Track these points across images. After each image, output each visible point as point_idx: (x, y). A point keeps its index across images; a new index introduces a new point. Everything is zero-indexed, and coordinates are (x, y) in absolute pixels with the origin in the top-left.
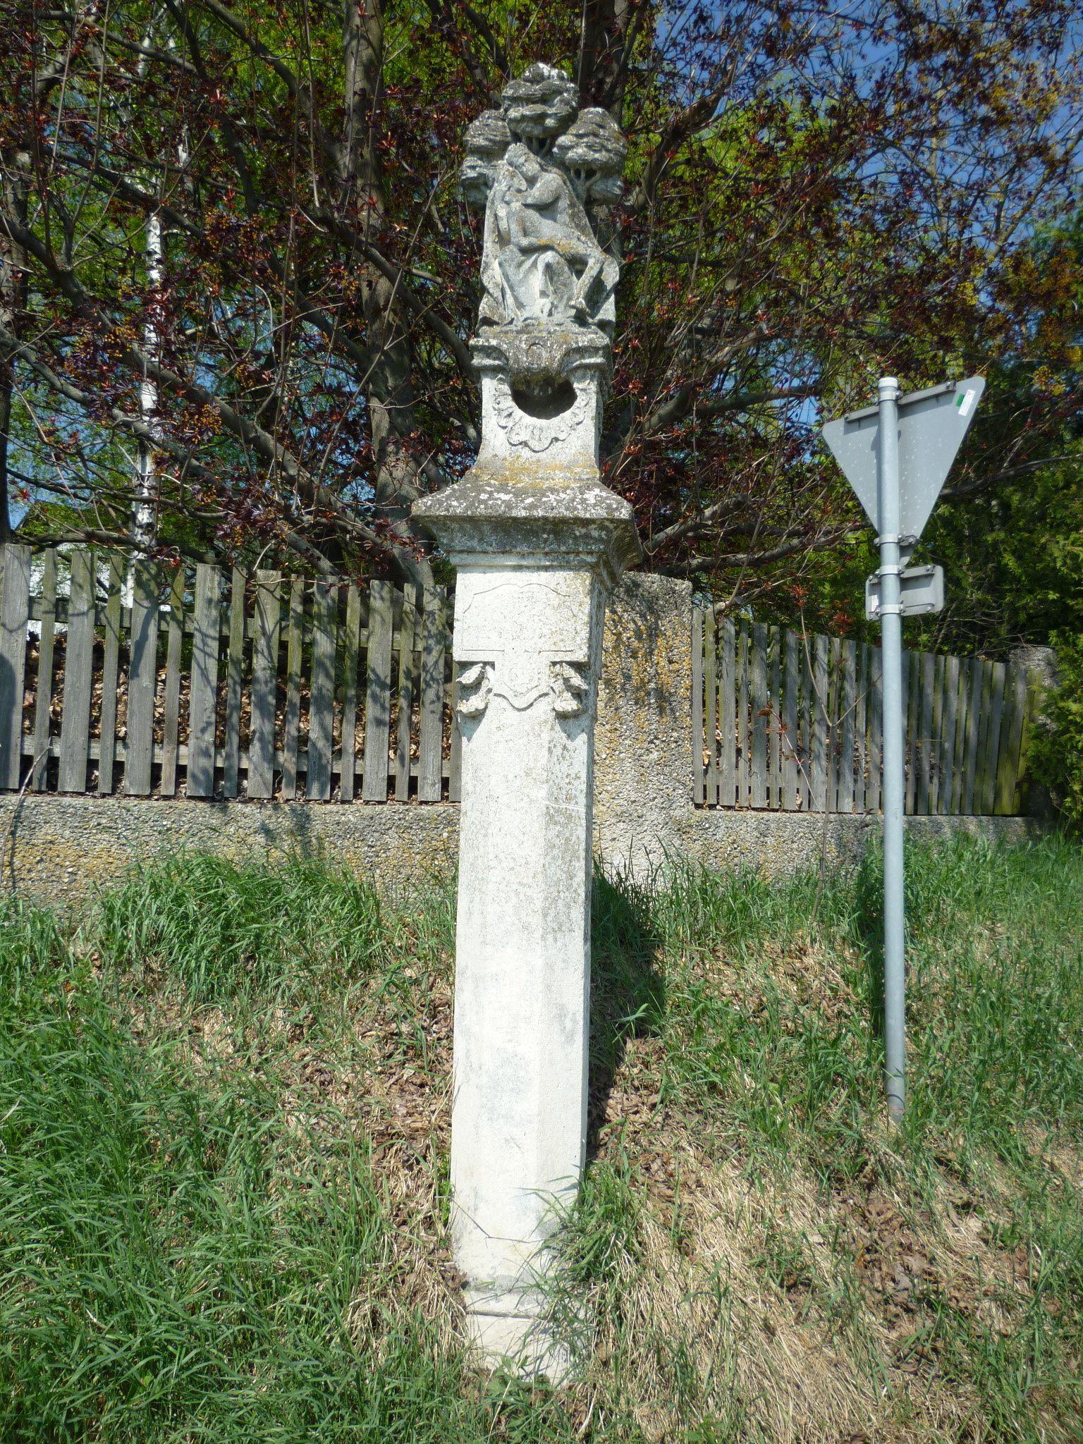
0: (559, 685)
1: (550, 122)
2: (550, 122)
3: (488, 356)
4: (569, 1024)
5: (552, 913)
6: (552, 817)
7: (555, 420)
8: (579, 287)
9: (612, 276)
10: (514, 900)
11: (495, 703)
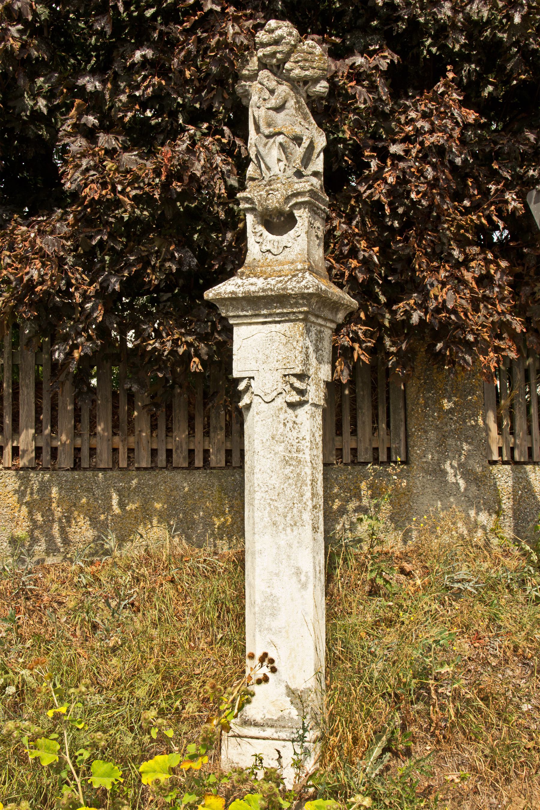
0: (288, 388)
1: (279, 56)
2: (279, 56)
3: (247, 202)
4: (303, 579)
5: (289, 515)
6: (287, 462)
7: (285, 236)
8: (299, 151)
9: (321, 142)
10: (268, 509)
11: (256, 400)
